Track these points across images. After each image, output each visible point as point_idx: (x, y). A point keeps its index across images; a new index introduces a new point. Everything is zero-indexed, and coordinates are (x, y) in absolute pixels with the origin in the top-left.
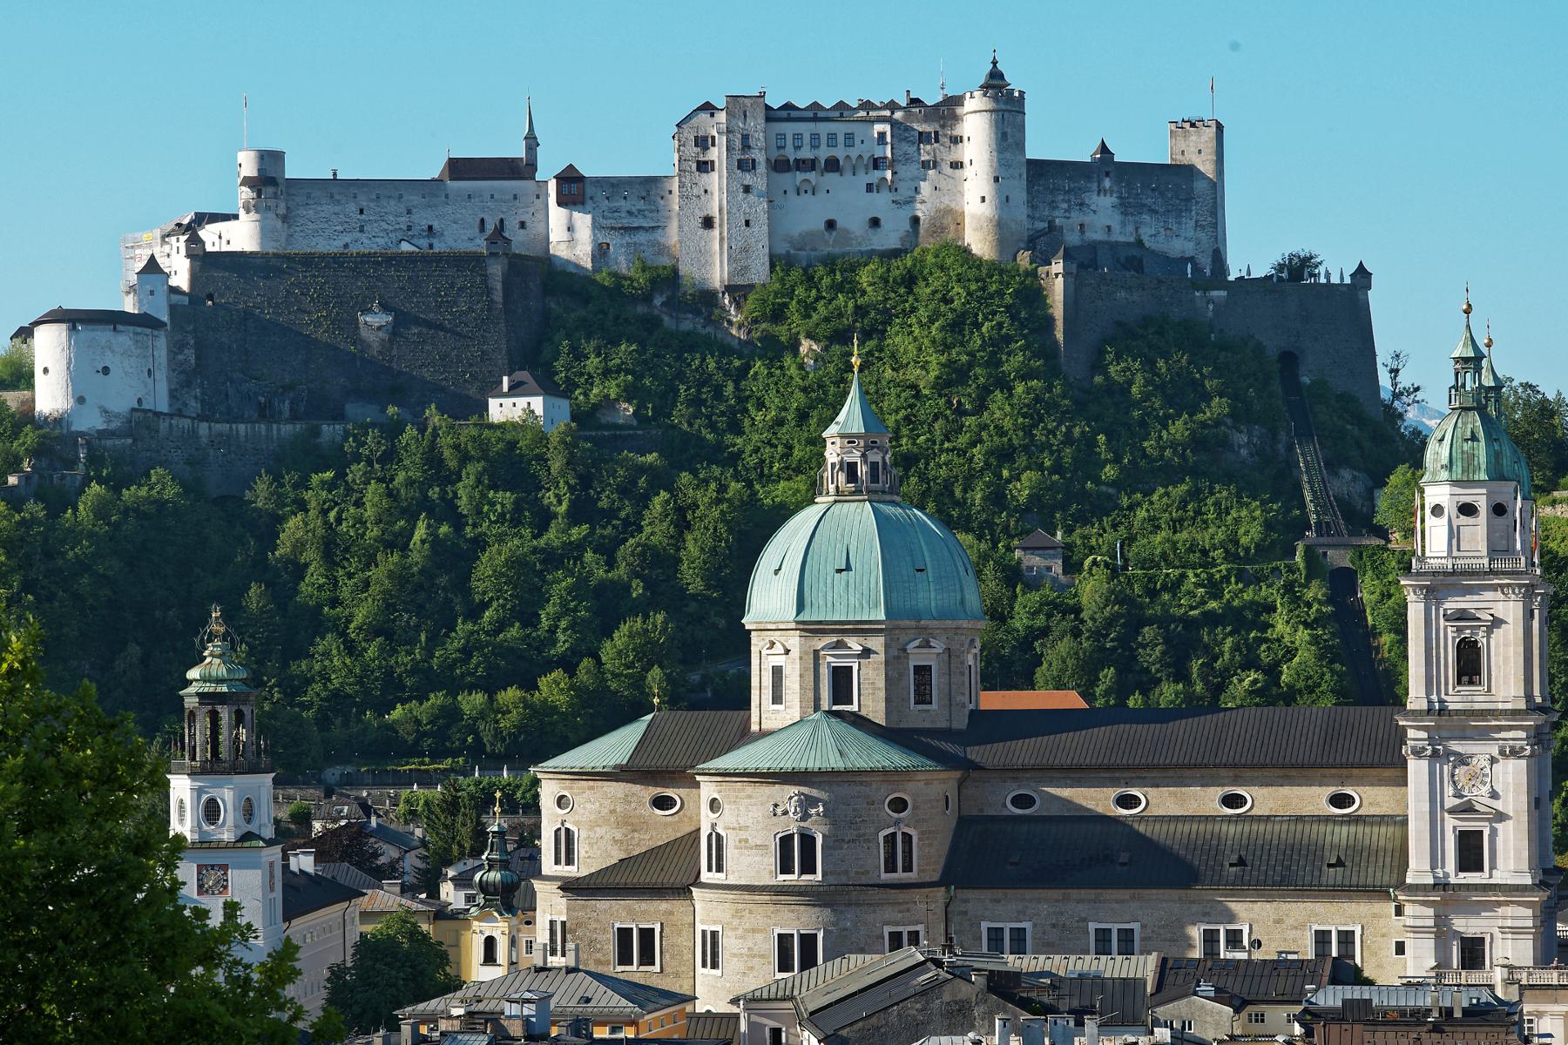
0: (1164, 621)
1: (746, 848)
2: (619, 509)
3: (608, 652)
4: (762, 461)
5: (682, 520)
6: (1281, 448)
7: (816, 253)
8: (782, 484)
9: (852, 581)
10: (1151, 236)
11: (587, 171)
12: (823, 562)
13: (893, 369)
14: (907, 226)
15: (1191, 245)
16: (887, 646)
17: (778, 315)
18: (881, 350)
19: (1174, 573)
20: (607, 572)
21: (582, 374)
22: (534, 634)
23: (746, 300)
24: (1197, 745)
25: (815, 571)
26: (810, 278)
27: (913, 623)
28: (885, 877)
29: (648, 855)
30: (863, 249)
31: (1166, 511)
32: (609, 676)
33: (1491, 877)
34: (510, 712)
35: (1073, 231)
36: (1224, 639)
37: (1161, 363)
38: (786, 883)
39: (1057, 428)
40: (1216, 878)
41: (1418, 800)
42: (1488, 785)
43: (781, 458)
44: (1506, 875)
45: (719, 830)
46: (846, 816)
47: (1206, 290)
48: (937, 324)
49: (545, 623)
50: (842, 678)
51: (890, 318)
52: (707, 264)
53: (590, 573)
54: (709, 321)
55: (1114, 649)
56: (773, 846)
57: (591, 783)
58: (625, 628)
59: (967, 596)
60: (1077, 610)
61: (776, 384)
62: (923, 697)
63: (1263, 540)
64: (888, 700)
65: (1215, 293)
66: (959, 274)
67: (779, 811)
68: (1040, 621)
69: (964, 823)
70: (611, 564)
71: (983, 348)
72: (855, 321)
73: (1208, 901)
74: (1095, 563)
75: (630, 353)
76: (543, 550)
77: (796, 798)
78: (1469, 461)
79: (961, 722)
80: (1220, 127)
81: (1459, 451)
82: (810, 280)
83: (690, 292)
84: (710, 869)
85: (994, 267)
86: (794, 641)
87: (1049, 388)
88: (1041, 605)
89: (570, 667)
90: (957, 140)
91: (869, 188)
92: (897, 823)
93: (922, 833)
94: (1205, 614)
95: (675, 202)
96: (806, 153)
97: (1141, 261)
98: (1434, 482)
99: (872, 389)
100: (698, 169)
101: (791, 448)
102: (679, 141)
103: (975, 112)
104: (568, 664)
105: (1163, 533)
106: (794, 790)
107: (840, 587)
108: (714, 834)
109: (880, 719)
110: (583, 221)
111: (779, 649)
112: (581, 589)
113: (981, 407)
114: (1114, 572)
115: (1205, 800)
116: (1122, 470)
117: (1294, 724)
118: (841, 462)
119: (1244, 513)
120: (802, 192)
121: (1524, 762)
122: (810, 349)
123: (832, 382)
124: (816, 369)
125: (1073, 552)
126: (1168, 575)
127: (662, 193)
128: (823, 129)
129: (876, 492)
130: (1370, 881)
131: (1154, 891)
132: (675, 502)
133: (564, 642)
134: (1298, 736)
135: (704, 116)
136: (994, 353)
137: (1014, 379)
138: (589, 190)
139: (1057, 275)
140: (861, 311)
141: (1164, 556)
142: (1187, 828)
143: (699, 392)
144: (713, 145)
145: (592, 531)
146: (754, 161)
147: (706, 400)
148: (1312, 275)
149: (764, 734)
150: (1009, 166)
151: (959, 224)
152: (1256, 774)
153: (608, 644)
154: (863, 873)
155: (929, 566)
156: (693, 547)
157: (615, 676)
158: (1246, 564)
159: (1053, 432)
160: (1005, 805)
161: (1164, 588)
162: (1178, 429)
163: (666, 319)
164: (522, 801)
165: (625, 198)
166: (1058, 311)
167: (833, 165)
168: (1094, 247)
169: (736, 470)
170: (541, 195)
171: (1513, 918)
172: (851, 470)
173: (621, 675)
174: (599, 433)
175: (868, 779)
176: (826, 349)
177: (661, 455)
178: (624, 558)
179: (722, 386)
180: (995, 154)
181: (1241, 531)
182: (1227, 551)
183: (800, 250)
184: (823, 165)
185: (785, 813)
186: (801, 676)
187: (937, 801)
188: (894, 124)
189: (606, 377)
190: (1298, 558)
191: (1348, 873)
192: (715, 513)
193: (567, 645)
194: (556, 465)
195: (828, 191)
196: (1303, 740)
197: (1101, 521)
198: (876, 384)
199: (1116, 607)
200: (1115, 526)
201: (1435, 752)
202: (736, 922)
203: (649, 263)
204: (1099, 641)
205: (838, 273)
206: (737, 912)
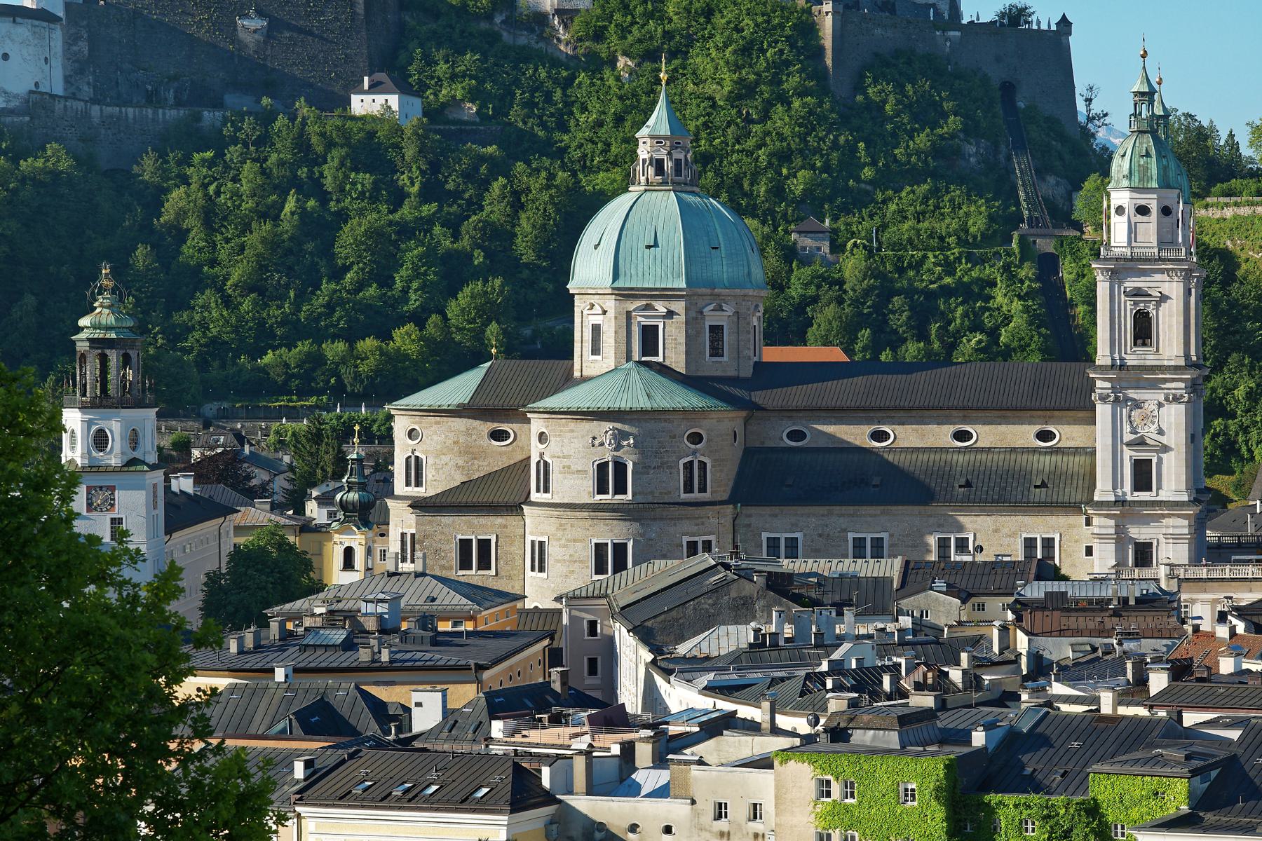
0: (909, 292)
2: (464, 191)
3: (453, 309)
5: (517, 202)
8: (602, 174)
13: (694, 84)
17: (599, 36)
18: (684, 68)
20: (453, 243)
31: (911, 205)
32: (454, 329)
36: (956, 307)
39: (826, 136)
48: (730, 49)
51: (692, 42)
53: (439, 243)
58: (467, 290)
61: (597, 92)
66: (748, 9)
70: (456, 236)
71: (767, 69)
72: (663, 43)
87: (820, 104)
89: (419, 319)
94: (940, 287)
99: (677, 99)
101: (608, 145)
105: (910, 223)
112: (430, 256)
113: (765, 117)
114: (870, 252)
115: (940, 435)
116: (878, 171)
117: (1010, 375)
119: (973, 208)
122: (626, 65)
126: (913, 256)
132: (512, 187)
136: (776, 74)
137: (792, 96)
140: (668, 35)
141: (910, 241)
145: (440, 208)
153: (453, 303)
157: (459, 329)
158: (974, 248)
159: (822, 139)
161: (910, 266)
162: (922, 140)
166: (828, 43)
169: (563, 162)
173: (464, 328)
176: (639, 65)
177: (499, 148)
178: (468, 232)
181: (971, 222)
182: (959, 238)
192: (546, 197)
197: (860, 212)
200: (871, 216)
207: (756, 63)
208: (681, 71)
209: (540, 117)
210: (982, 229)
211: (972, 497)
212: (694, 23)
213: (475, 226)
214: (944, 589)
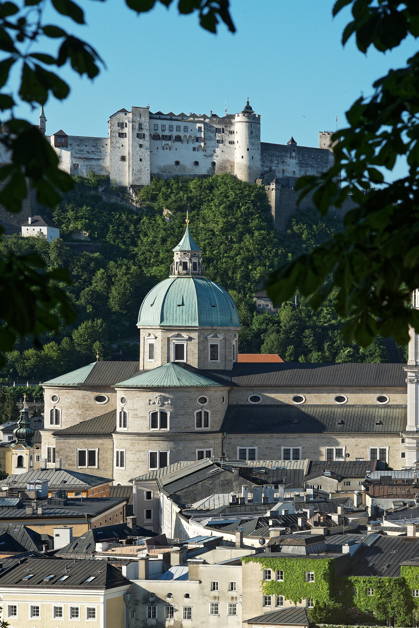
1: (137, 418)
7: (171, 174)
13: (203, 223)
18: (198, 215)
30: (191, 174)
38: (154, 432)
45: (125, 411)
46: (180, 405)
51: (202, 202)
67: (151, 403)
72: (187, 203)
77: (159, 397)
79: (230, 367)
84: (120, 426)
91: (194, 149)
92: (202, 408)
99: (194, 231)
106: (157, 394)
108: (123, 412)
123: (177, 227)
140: (190, 199)
175: (190, 390)
176: (174, 213)
185: (154, 403)
187: (219, 399)
188: (205, 124)
195: (176, 149)
198: (196, 229)
205: (180, 183)
208: (196, 217)
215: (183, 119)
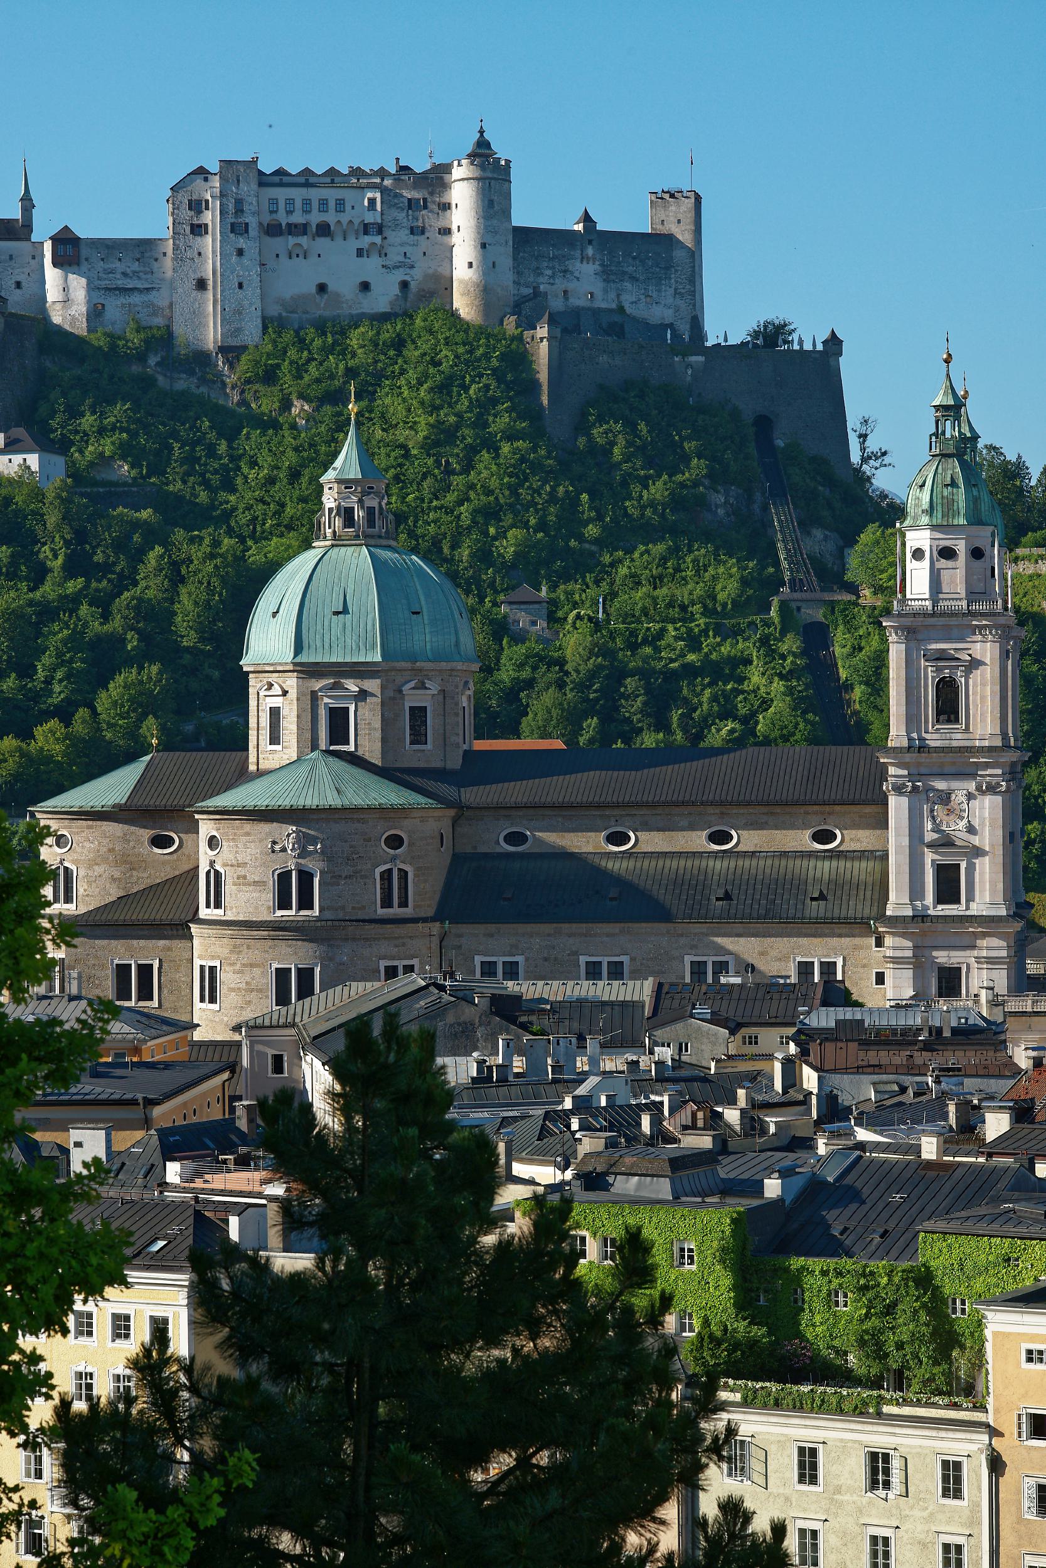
0: (644, 674)
1: (244, 884)
2: (114, 564)
3: (103, 701)
4: (255, 518)
5: (176, 576)
6: (756, 507)
9: (348, 624)
10: (632, 303)
11: (82, 232)
12: (320, 606)
13: (383, 430)
14: (396, 290)
15: (670, 312)
16: (383, 688)
17: (270, 376)
18: (371, 412)
19: (655, 627)
20: (101, 624)
21: (77, 432)
22: (30, 685)
23: (239, 361)
24: (684, 783)
25: (313, 611)
26: (302, 341)
27: (408, 665)
28: (381, 912)
29: (146, 892)
30: (354, 312)
31: (646, 568)
32: (104, 726)
33: (968, 908)
34: (6, 761)
35: (556, 296)
36: (703, 690)
37: (642, 427)
40: (703, 912)
41: (897, 835)
42: (965, 821)
43: (274, 514)
44: (982, 907)
45: (218, 867)
47: (684, 355)
48: (425, 386)
49: (41, 674)
50: (338, 721)
51: (380, 380)
52: (204, 325)
53: (86, 625)
54: (203, 381)
55: (597, 700)
56: (271, 882)
57: (90, 823)
58: (120, 679)
59: (462, 639)
60: (561, 662)
62: (418, 737)
63: (740, 596)
64: (384, 740)
65: (693, 359)
66: (446, 338)
67: (277, 847)
68: (526, 674)
69: (458, 859)
70: (106, 617)
71: (470, 409)
73: (695, 934)
74: (578, 617)
75: (125, 411)
76: (39, 603)
78: (949, 506)
79: (455, 762)
80: (698, 198)
81: (939, 496)
82: (302, 343)
83: (183, 352)
84: (208, 906)
85: (481, 331)
86: (291, 682)
87: (534, 449)
88: (527, 657)
90: (446, 207)
91: (360, 253)
92: (393, 859)
93: (417, 869)
94: (685, 666)
95: (168, 263)
96: (298, 218)
97: (622, 327)
98: (915, 527)
100: (192, 232)
101: (283, 505)
102: (173, 204)
103: (463, 179)
104: (64, 713)
105: (644, 589)
107: (336, 630)
109: (378, 762)
110: (78, 285)
111: (277, 690)
113: (468, 467)
116: (604, 528)
118: (339, 507)
119: (721, 570)
120: (294, 256)
121: (999, 799)
122: (302, 410)
124: (308, 429)
125: (557, 607)
126: (648, 629)
127: (156, 256)
128: (315, 194)
129: (372, 537)
130: (851, 913)
131: (644, 925)
132: (170, 557)
133: (60, 693)
134: (782, 774)
135: (199, 181)
136: (480, 416)
137: (501, 440)
138: (84, 252)
139: (542, 339)
140: (351, 373)
141: (645, 612)
142: (675, 864)
143: (193, 450)
144: (207, 208)
145: (87, 586)
146: (247, 224)
147: (200, 458)
148: (786, 342)
149: (261, 774)
150: (496, 233)
151: (449, 289)
152: (742, 811)
154: (359, 909)
155: (425, 610)
156: (187, 602)
157: (111, 726)
160: (498, 843)
161: (645, 642)
162: (658, 490)
163: (160, 378)
164: (18, 848)
165: (120, 260)
166: (543, 376)
167: (324, 230)
168: (577, 312)
170: (38, 256)
171: (988, 948)
172: (347, 515)
173: (115, 725)
174: (95, 490)
176: (317, 409)
177: (156, 511)
178: (119, 611)
179: (216, 444)
180: (481, 220)
181: (719, 587)
182: (705, 606)
183: (292, 312)
184: (314, 230)
185: (284, 850)
186: (298, 717)
188: (384, 191)
189: (101, 434)
190: (773, 613)
191: (830, 906)
192: (210, 568)
193: (62, 696)
194: (52, 520)
196: (787, 778)
197: (584, 578)
199: (600, 659)
200: (597, 583)
201: (915, 789)
202: (234, 957)
203: (144, 324)
204: (583, 692)
205: (329, 335)
206: (235, 946)
207: (456, 403)
208: (367, 415)
209: (203, 475)
210: (733, 595)
211: (733, 911)
212: (382, 357)
213: (128, 605)
214: (709, 1016)
215: (333, 181)
